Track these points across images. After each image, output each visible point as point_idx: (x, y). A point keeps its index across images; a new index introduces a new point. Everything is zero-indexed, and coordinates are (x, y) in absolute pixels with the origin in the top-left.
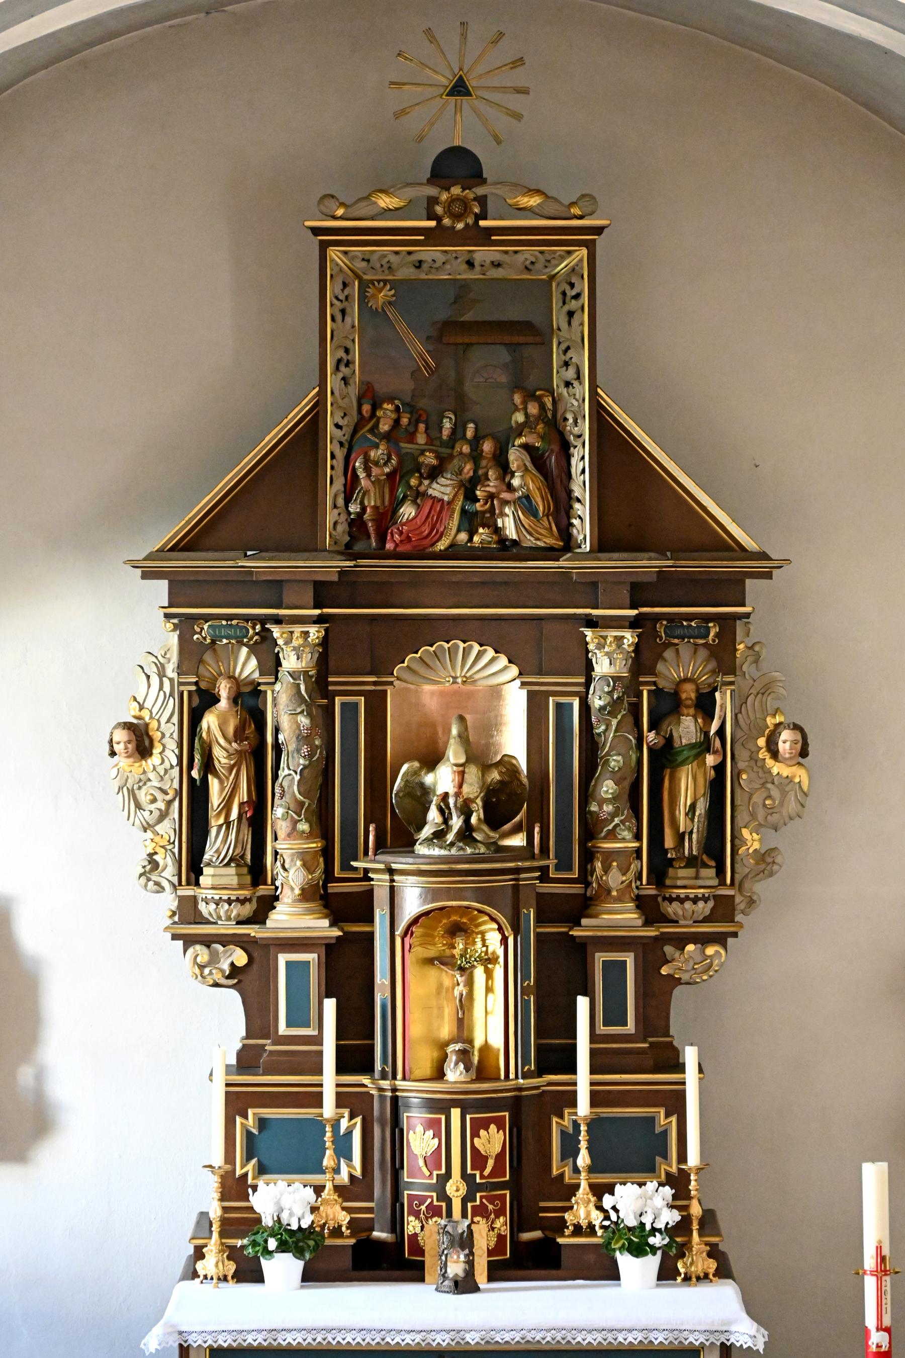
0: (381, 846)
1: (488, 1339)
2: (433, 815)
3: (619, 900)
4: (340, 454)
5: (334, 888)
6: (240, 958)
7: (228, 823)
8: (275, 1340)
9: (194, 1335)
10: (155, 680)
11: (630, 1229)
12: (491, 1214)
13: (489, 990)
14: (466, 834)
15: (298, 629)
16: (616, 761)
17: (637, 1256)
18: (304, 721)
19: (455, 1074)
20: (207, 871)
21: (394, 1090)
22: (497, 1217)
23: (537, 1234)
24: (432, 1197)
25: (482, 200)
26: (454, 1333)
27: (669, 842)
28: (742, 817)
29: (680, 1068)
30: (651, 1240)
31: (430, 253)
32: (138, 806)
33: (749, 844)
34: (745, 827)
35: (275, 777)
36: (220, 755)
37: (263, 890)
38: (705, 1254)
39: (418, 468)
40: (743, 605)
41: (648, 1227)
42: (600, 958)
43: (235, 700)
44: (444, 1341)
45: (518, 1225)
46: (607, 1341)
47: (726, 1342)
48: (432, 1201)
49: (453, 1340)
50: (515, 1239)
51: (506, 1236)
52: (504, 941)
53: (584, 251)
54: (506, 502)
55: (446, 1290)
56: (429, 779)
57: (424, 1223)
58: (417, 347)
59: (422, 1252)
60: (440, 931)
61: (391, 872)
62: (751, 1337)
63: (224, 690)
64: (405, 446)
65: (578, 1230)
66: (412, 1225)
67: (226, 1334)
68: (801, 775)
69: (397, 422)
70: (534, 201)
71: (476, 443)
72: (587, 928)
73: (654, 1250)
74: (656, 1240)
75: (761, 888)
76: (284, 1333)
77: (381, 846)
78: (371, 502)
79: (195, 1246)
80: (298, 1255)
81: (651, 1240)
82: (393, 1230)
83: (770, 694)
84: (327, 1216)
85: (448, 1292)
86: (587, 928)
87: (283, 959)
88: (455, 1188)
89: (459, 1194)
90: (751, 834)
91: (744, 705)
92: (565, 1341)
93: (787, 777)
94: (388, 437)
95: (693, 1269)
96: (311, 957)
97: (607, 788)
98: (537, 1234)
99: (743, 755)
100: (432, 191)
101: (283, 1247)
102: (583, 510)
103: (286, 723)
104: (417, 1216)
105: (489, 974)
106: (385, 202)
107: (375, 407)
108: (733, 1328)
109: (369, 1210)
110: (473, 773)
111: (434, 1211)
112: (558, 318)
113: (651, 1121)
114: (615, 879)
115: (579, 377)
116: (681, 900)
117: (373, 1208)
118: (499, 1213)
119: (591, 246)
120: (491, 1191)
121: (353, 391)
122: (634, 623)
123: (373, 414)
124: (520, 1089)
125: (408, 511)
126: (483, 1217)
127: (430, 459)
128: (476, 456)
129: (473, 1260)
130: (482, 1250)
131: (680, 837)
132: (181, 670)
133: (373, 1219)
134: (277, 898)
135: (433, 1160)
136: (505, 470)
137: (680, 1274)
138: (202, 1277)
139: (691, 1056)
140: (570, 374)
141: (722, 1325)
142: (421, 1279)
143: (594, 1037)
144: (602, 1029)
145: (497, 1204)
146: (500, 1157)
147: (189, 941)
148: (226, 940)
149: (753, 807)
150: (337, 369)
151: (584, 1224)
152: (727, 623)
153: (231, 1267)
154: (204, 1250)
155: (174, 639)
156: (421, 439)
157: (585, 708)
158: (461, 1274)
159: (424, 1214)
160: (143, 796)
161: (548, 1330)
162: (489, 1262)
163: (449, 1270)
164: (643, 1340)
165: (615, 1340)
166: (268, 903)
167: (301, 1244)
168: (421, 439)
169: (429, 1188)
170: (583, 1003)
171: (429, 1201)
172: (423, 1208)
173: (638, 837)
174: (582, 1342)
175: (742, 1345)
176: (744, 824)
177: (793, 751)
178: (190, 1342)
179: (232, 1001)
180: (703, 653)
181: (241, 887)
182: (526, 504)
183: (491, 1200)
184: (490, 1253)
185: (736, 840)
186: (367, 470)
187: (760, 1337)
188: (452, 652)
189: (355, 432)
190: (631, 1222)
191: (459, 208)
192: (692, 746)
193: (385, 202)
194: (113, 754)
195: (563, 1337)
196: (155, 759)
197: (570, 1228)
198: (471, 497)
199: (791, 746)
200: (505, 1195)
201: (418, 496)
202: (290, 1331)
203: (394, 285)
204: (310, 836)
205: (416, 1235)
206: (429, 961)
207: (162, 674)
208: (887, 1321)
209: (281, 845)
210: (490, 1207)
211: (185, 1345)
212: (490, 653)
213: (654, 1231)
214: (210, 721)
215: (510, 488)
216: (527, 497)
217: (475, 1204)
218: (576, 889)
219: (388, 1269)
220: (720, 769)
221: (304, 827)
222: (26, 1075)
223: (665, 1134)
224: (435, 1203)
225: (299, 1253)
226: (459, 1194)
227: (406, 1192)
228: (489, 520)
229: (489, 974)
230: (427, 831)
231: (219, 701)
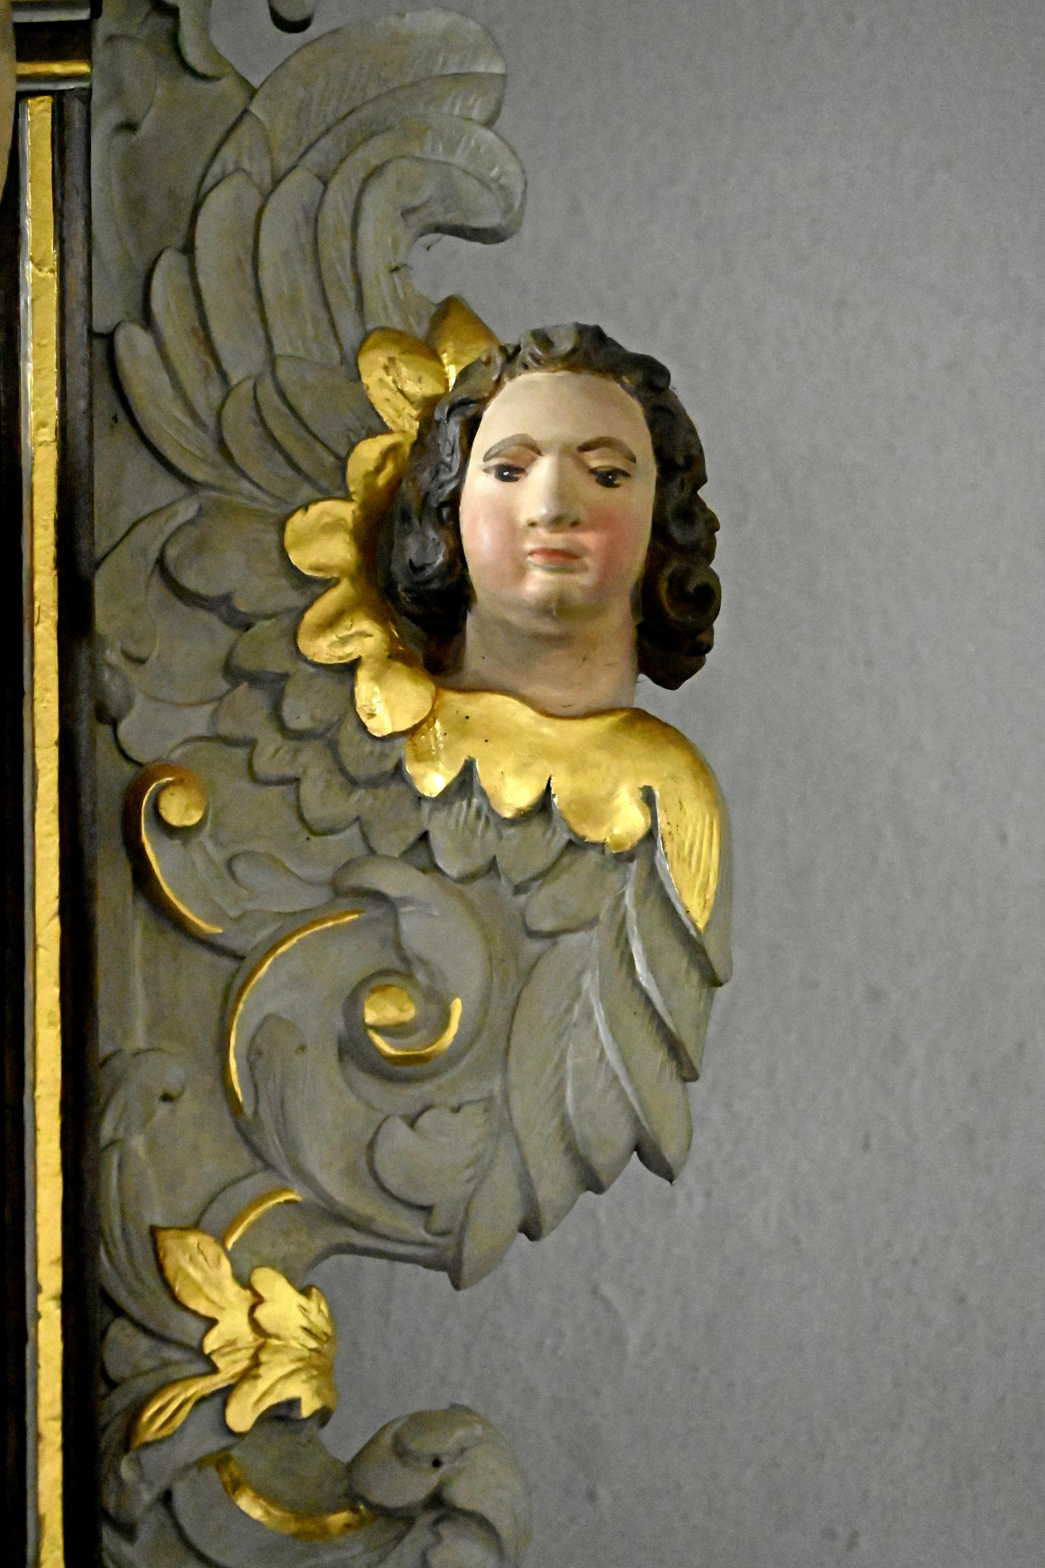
33: (229, 1368)
34: (196, 1226)
83: (376, 172)
90: (245, 1282)
91: (170, 264)
93: (544, 805)
149: (253, 1056)
176: (187, 1206)
177: (588, 539)
185: (119, 1333)
199: (561, 492)
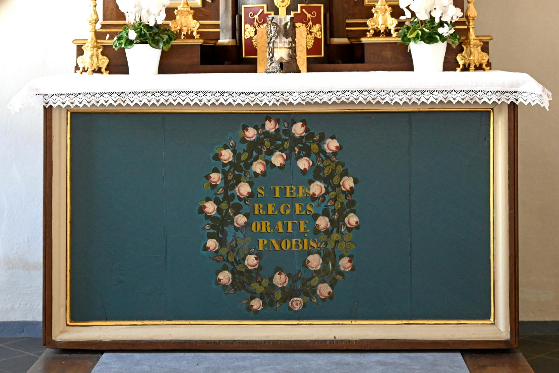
1: (308, 100)
8: (124, 102)
9: (54, 97)
11: (423, 23)
12: (309, 22)
17: (429, 43)
22: (314, 24)
23: (344, 41)
24: (263, 8)
26: (279, 94)
30: (440, 30)
38: (479, 48)
41: (437, 21)
44: (270, 102)
45: (330, 32)
46: (412, 101)
47: (515, 102)
48: (263, 11)
49: (278, 101)
50: (328, 43)
51: (321, 39)
55: (273, 70)
57: (257, 28)
59: (255, 52)
62: (537, 95)
65: (377, 33)
66: (248, 31)
67: (81, 96)
73: (443, 39)
74: (445, 31)
76: (131, 95)
79: (78, 46)
80: (154, 45)
81: (440, 30)
82: (234, 37)
84: (181, 24)
85: (274, 72)
89: (284, 4)
92: (376, 101)
95: (472, 58)
101: (142, 39)
104: (252, 24)
108: (520, 90)
109: (217, 26)
111: (263, 18)
117: (219, 25)
118: (316, 21)
120: (308, 4)
126: (303, 23)
129: (295, 47)
130: (303, 47)
133: (218, 33)
137: (459, 66)
138: (81, 70)
141: (512, 87)
142: (255, 71)
145: (314, 13)
151: (382, 28)
153: (104, 62)
154: (83, 48)
158: (286, 58)
159: (257, 21)
161: (361, 92)
162: (308, 58)
163: (275, 55)
164: (443, 100)
165: (419, 100)
167: (157, 38)
171: (261, 11)
172: (256, 17)
174: (390, 102)
175: (530, 103)
178: (51, 103)
183: (310, 10)
184: (309, 52)
187: (545, 96)
190: (426, 17)
195: (374, 97)
197: (371, 31)
200: (320, 7)
202: (136, 93)
205: (251, 38)
210: (309, 16)
211: (47, 106)
213: (441, 24)
217: (297, 12)
219: (229, 64)
224: (266, 12)
225: (155, 44)
226: (284, 4)
227: (243, 6)
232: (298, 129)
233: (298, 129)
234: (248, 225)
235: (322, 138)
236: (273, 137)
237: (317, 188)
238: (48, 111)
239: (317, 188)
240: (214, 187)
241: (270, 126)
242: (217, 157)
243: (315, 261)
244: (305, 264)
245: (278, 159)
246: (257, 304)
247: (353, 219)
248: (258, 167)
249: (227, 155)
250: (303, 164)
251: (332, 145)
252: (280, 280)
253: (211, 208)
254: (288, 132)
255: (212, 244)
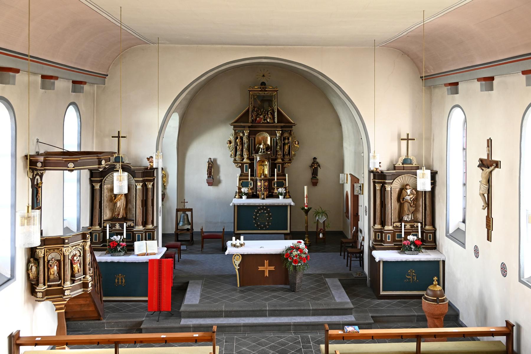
0: (255, 153)
2: (260, 150)
3: (279, 159)
4: (251, 113)
5: (250, 157)
6: (240, 165)
7: (239, 151)
10: (232, 136)
13: (266, 168)
14: (264, 152)
15: (247, 131)
16: (279, 144)
18: (247, 140)
19: (262, 177)
20: (237, 156)
21: (256, 178)
23: (271, 193)
25: (266, 87)
27: (285, 153)
28: (292, 150)
29: (286, 176)
31: (261, 92)
32: (230, 149)
35: (244, 146)
36: (238, 144)
37: (243, 158)
39: (259, 114)
40: (292, 128)
42: (278, 165)
43: (240, 138)
45: (269, 192)
52: (268, 163)
53: (276, 92)
54: (268, 118)
56: (260, 146)
58: (259, 102)
60: (261, 162)
61: (256, 156)
63: (239, 137)
64: (258, 112)
65: (275, 193)
66: (258, 192)
68: (298, 146)
69: (257, 110)
70: (271, 87)
71: (265, 112)
72: (276, 162)
73: (283, 195)
74: (283, 194)
75: (294, 158)
77: (255, 153)
78: (254, 118)
86: (276, 162)
87: (245, 165)
88: (262, 189)
94: (256, 111)
96: (248, 165)
97: (278, 147)
98: (271, 193)
99: (292, 144)
100: (261, 86)
101: (245, 195)
102: (276, 119)
103: (245, 140)
105: (266, 166)
106: (256, 87)
107: (255, 108)
110: (265, 146)
111: (260, 191)
112: (273, 99)
113: (283, 182)
114: (279, 157)
115: (276, 105)
116: (286, 159)
118: (267, 191)
119: (277, 92)
121: (252, 106)
122: (281, 130)
123: (254, 109)
124: (269, 178)
125: (258, 119)
127: (260, 113)
128: (265, 113)
131: (286, 152)
132: (234, 135)
134: (244, 159)
135: (260, 186)
136: (268, 115)
139: (287, 175)
140: (275, 105)
142: (259, 198)
143: (277, 173)
144: (278, 172)
146: (267, 185)
147: (235, 163)
148: (239, 163)
150: (251, 104)
152: (291, 130)
153: (239, 197)
155: (234, 132)
156: (259, 111)
157: (276, 139)
160: (230, 148)
166: (243, 159)
168: (259, 111)
169: (260, 189)
170: (276, 169)
173: (281, 152)
179: (240, 169)
180: (288, 134)
181: (240, 157)
182: (270, 118)
184: (266, 195)
186: (254, 115)
188: (262, 133)
189: (253, 111)
190: (281, 192)
191: (263, 88)
192: (287, 143)
193: (256, 87)
194: (227, 144)
196: (232, 144)
198: (264, 117)
201: (259, 117)
203: (257, 96)
204: (247, 152)
206: (260, 165)
207: (233, 135)
208: (307, 202)
209: (245, 153)
212: (266, 133)
213: (283, 193)
214: (237, 140)
215: (269, 117)
216: (270, 117)
218: (275, 158)
220: (290, 145)
221: (247, 151)
222: (218, 177)
223: (284, 183)
225: (246, 195)
228: (266, 120)
229: (266, 166)
230: (260, 152)
231: (238, 138)
232: (265, 207)
233: (265, 207)
234: (258, 219)
235: (268, 208)
236: (261, 208)
237: (267, 215)
238: (234, 205)
239: (267, 215)
240: (254, 214)
241: (261, 207)
242: (255, 211)
243: (267, 223)
244: (265, 224)
245: (262, 211)
246: (259, 228)
247: (271, 218)
248: (260, 212)
249: (256, 211)
250: (265, 212)
251: (269, 209)
252: (262, 226)
253: (254, 217)
254: (263, 208)
255: (254, 221)
